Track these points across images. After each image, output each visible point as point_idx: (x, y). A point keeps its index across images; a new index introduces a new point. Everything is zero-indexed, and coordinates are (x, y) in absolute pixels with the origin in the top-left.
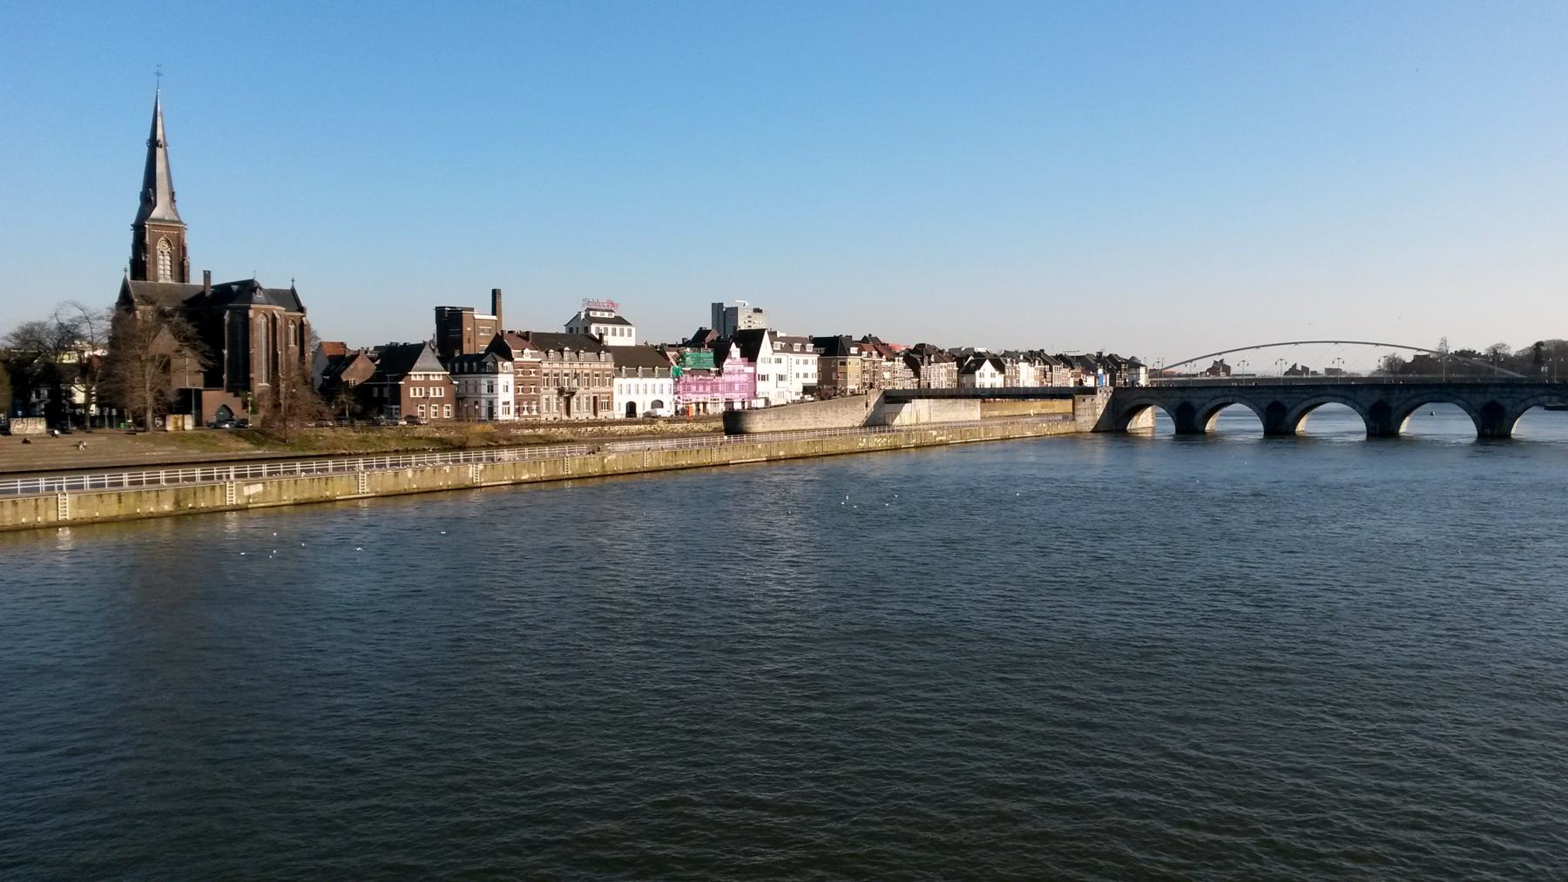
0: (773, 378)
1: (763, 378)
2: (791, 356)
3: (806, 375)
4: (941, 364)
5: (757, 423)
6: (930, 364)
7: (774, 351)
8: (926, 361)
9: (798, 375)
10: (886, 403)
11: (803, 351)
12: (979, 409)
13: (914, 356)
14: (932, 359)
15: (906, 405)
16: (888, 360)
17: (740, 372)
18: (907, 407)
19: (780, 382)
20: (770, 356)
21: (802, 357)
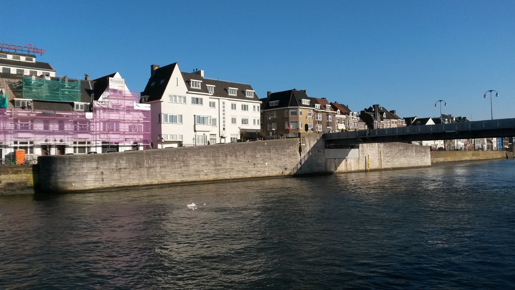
0: (189, 121)
1: (173, 119)
2: (222, 100)
3: (245, 121)
4: (392, 120)
5: (86, 175)
6: (382, 119)
7: (189, 89)
8: (379, 116)
9: (234, 121)
10: (326, 148)
11: (241, 95)
12: (430, 155)
13: (368, 113)
14: (384, 116)
15: (353, 150)
16: (342, 113)
17: (130, 110)
18: (353, 153)
19: (199, 127)
20: (185, 95)
21: (239, 104)
